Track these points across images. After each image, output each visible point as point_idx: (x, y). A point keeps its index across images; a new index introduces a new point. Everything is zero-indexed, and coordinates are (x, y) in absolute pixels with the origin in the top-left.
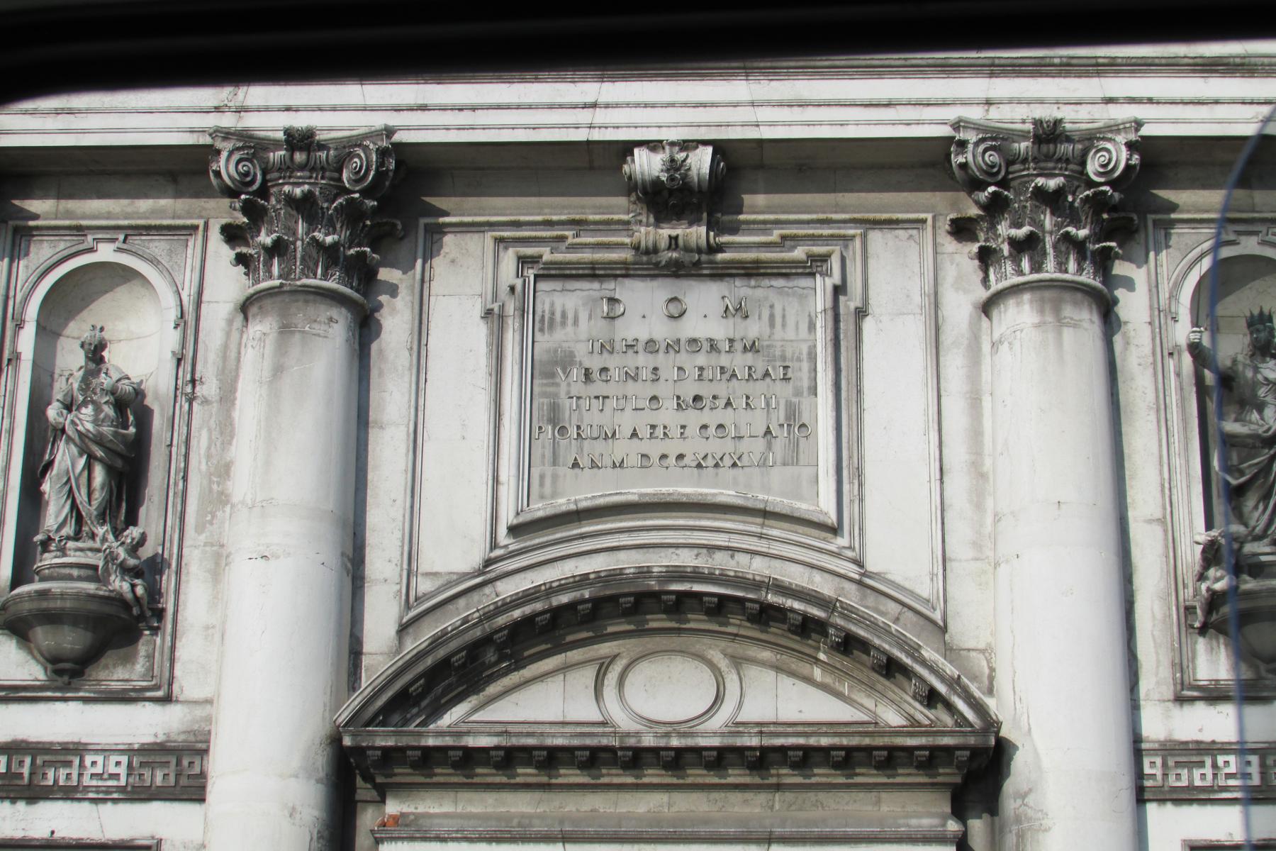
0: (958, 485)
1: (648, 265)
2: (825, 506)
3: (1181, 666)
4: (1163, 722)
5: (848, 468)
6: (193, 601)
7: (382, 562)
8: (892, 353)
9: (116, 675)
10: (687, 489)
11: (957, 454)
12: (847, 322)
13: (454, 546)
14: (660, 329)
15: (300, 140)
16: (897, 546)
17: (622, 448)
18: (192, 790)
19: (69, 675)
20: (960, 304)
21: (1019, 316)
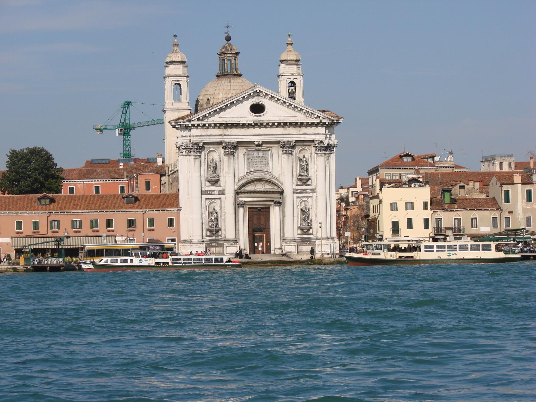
0: (280, 168)
1: (256, 150)
2: (270, 170)
3: (297, 183)
4: (296, 187)
5: (272, 167)
6: (222, 179)
7: (236, 175)
8: (275, 156)
9: (217, 185)
10: (260, 169)
11: (280, 166)
12: (272, 155)
13: (242, 174)
14: (257, 156)
15: (230, 143)
16: (275, 174)
17: (255, 166)
18: (223, 194)
19: (213, 185)
20: (281, 153)
21: (285, 156)
